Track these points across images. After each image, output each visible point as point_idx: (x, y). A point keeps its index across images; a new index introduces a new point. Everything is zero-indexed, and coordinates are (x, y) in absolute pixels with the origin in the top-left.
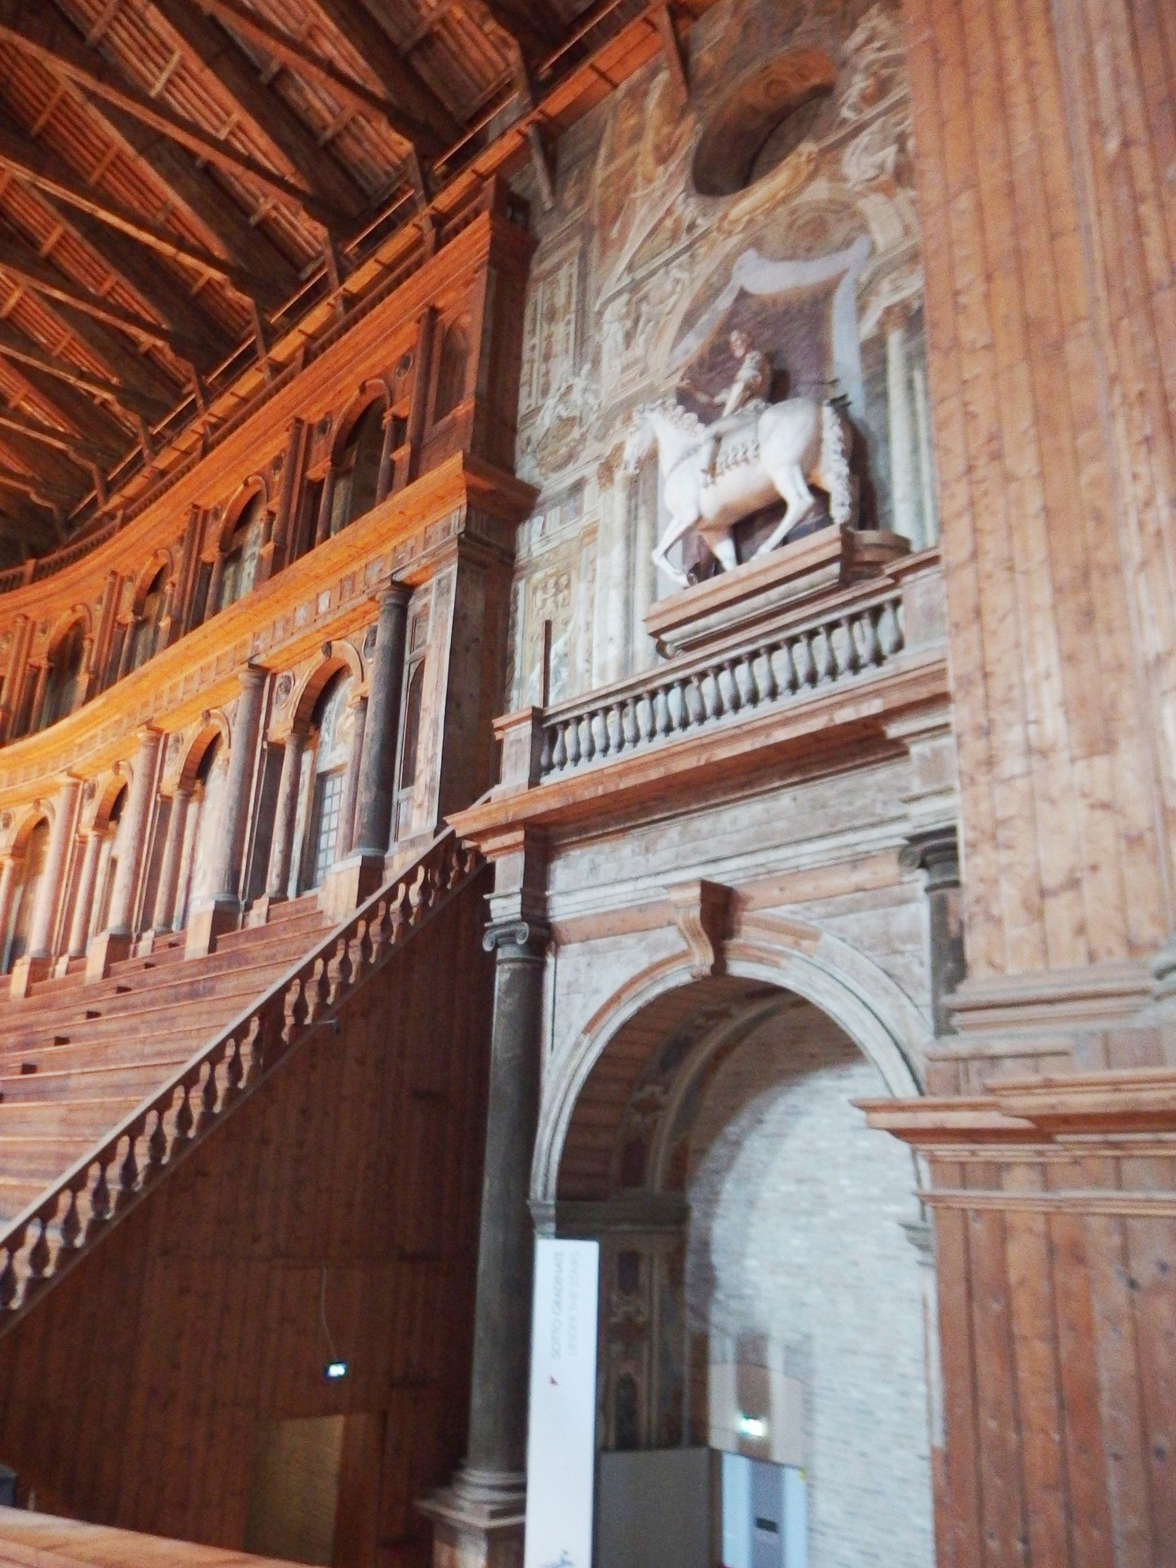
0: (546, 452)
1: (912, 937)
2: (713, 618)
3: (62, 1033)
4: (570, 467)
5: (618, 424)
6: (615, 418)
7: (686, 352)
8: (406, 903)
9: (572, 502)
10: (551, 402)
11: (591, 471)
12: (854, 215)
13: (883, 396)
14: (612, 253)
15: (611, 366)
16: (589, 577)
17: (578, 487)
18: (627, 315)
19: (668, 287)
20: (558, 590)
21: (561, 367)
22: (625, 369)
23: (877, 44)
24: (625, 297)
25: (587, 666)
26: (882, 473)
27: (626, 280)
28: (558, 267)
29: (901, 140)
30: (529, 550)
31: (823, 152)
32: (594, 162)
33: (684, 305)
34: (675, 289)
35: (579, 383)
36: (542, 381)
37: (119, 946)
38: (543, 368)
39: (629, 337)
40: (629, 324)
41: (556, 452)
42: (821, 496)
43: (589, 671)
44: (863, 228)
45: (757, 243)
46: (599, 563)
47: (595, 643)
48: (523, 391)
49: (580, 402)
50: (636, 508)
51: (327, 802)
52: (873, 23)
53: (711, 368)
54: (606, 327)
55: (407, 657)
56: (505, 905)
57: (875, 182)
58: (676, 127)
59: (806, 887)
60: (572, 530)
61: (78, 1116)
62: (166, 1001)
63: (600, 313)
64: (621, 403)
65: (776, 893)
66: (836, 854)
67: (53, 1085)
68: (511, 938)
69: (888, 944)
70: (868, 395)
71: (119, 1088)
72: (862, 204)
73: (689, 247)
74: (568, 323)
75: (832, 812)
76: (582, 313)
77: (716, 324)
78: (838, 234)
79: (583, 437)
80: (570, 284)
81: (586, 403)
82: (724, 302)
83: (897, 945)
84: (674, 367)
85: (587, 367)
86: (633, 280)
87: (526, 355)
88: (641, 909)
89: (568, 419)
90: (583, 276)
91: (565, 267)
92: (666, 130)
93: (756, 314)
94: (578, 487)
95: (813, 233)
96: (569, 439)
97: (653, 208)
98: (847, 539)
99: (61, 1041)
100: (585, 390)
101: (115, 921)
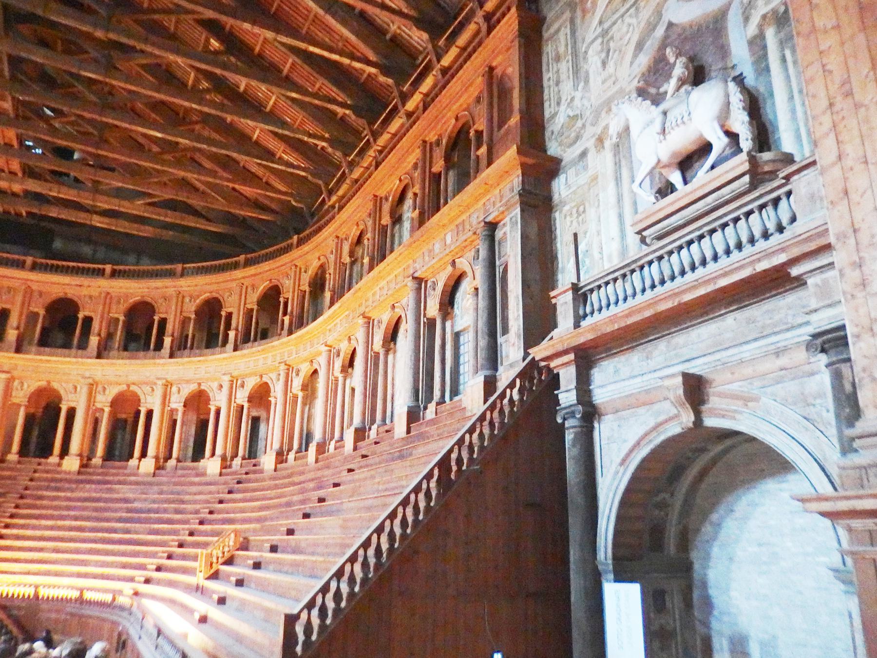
1: (821, 395)
3: (336, 481)
5: (603, 114)
7: (639, 65)
8: (511, 400)
10: (563, 108)
13: (767, 69)
14: (588, 16)
15: (595, 81)
16: (596, 204)
17: (584, 154)
18: (602, 51)
20: (579, 215)
21: (567, 87)
22: (603, 82)
24: (600, 40)
25: (600, 256)
26: (771, 116)
27: (599, 30)
28: (558, 31)
33: (635, 38)
34: (629, 29)
37: (360, 434)
38: (556, 89)
39: (604, 64)
40: (603, 55)
41: (569, 136)
42: (733, 137)
43: (602, 258)
46: (601, 195)
47: (603, 242)
48: (546, 105)
49: (579, 106)
51: (462, 348)
55: (497, 263)
56: (567, 396)
59: (748, 371)
61: (350, 524)
62: (387, 461)
63: (586, 52)
65: (729, 375)
66: (766, 349)
67: (334, 508)
68: (572, 415)
69: (805, 401)
70: (756, 70)
71: (369, 509)
74: (568, 61)
75: (760, 324)
76: (575, 54)
77: (656, 47)
79: (584, 126)
82: (660, 32)
83: (810, 400)
85: (582, 84)
88: (647, 392)
90: (573, 32)
93: (680, 35)
94: (584, 154)
98: (752, 160)
99: (336, 485)
101: (357, 421)
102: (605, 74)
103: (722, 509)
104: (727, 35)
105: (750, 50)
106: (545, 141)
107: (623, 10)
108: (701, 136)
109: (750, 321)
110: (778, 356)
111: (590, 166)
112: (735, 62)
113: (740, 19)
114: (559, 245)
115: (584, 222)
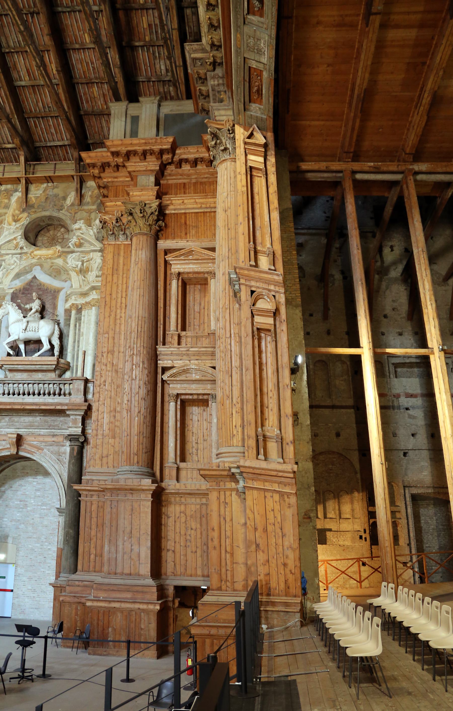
1: (65, 453)
2: (20, 366)
7: (16, 284)
12: (68, 274)
13: (69, 325)
19: (13, 262)
26: (66, 344)
29: (83, 262)
31: (63, 252)
33: (17, 270)
45: (41, 266)
52: (81, 225)
53: (23, 293)
58: (21, 213)
59: (41, 439)
69: (59, 454)
70: (65, 323)
72: (70, 272)
73: (20, 254)
77: (26, 281)
78: (64, 277)
82: (29, 277)
83: (61, 454)
84: (12, 287)
92: (17, 212)
93: (38, 285)
95: (57, 272)
97: (10, 234)
98: (58, 359)
103: (7, 486)
104: (58, 301)
112: (58, 314)
113: (64, 299)
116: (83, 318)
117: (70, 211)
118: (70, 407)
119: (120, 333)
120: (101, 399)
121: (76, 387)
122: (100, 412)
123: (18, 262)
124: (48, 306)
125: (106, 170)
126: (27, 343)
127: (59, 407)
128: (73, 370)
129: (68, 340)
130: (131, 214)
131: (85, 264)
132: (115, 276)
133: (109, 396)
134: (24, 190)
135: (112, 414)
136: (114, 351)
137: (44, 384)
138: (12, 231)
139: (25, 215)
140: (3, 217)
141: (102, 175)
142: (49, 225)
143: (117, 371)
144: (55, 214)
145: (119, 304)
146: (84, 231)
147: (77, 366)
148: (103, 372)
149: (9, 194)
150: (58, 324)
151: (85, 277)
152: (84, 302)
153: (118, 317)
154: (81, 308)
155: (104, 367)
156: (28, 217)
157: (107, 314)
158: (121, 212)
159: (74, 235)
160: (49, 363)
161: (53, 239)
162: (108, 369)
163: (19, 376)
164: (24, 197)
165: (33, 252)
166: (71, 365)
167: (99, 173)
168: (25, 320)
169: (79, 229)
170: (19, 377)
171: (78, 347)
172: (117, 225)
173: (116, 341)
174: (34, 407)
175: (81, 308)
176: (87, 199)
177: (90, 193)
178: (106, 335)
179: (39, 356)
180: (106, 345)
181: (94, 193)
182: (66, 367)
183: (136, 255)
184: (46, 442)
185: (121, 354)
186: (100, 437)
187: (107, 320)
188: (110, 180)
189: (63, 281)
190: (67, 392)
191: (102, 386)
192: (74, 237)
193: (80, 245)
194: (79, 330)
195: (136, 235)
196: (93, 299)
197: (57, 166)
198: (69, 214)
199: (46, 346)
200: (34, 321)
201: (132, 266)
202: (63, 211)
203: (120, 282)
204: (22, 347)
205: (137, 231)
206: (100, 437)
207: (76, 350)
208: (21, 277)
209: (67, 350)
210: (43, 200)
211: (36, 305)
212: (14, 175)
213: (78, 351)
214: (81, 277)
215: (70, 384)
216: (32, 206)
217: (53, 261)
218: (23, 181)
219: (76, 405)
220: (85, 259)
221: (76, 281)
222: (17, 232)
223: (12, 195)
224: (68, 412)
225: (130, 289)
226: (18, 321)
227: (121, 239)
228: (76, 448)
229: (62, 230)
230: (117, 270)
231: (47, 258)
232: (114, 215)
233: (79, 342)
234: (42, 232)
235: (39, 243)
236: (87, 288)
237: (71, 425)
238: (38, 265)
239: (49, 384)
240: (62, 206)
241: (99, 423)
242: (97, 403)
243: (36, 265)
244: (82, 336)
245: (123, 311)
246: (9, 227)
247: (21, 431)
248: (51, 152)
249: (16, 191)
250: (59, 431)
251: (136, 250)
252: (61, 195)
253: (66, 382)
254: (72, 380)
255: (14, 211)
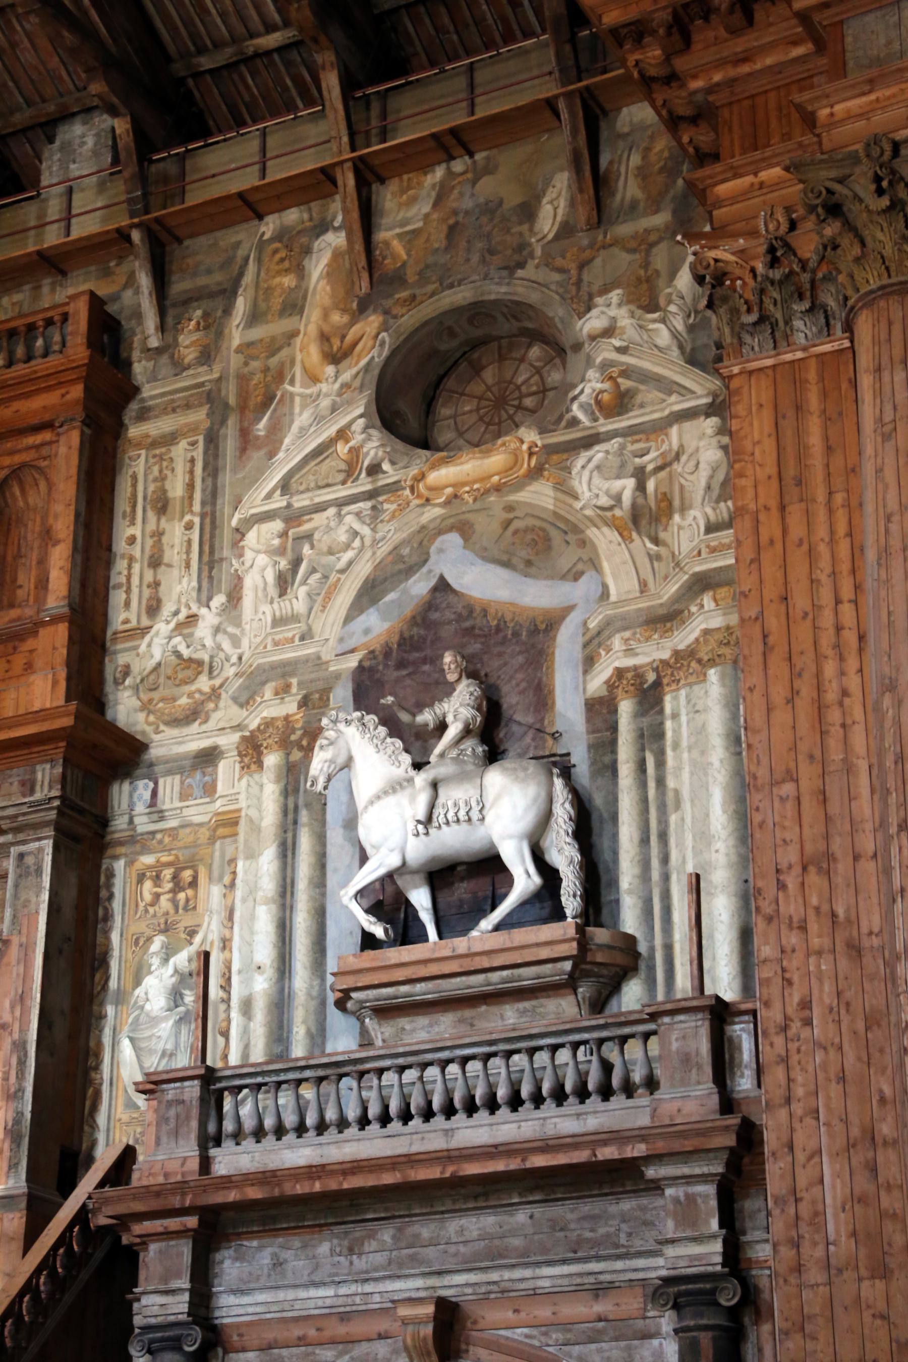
0: (156, 695)
4: (195, 727)
5: (268, 692)
6: (264, 683)
7: (367, 631)
9: (198, 775)
10: (162, 628)
11: (229, 741)
12: (583, 543)
14: (256, 456)
15: (257, 609)
16: (227, 880)
17: (208, 758)
18: (281, 551)
19: (343, 538)
20: (178, 887)
21: (179, 587)
22: (278, 622)
23: (617, 343)
24: (277, 525)
25: (222, 994)
26: (607, 856)
27: (278, 502)
28: (171, 439)
29: (641, 476)
30: (131, 821)
31: (551, 450)
32: (228, 311)
33: (364, 569)
34: (352, 541)
35: (208, 618)
36: (147, 593)
38: (149, 576)
39: (284, 583)
40: (284, 564)
41: (174, 699)
42: (550, 875)
43: (227, 1001)
44: (594, 564)
45: (464, 529)
46: (240, 864)
47: (235, 967)
48: (117, 598)
49: (209, 642)
50: (296, 809)
52: (613, 312)
53: (400, 665)
54: (249, 555)
57: (609, 514)
58: (352, 323)
59: (544, 1312)
60: (199, 812)
64: (273, 667)
65: (510, 1314)
66: (579, 1280)
70: (593, 763)
72: (592, 533)
73: (371, 495)
74: (189, 527)
75: (574, 1235)
76: (211, 521)
77: (408, 610)
78: (566, 559)
79: (215, 694)
80: (191, 472)
81: (219, 648)
82: (419, 587)
84: (351, 644)
85: (219, 600)
86: (289, 506)
87: (120, 546)
88: (344, 1317)
89: (190, 660)
90: (213, 470)
91: (183, 444)
92: (337, 318)
93: (460, 618)
94: (208, 758)
95: (535, 545)
96: (193, 688)
97: (319, 419)
100: (217, 630)
102: (284, 607)
104: (551, 668)
105: (589, 720)
106: (101, 681)
107: (343, 492)
108: (493, 846)
109: (556, 1226)
110: (597, 1296)
111: (220, 788)
112: (559, 726)
113: (578, 653)
114: (115, 937)
115: (190, 907)
116: (669, 725)
117: (559, 262)
118: (661, 1146)
119: (849, 769)
120: (800, 1092)
121: (675, 1046)
122: (801, 1157)
123: (366, 531)
124: (513, 700)
125: (696, 37)
126: (441, 875)
127: (608, 1153)
128: (652, 968)
129: (615, 836)
130: (834, 210)
131: (651, 485)
132: (795, 512)
133: (833, 1070)
134: (355, 215)
135: (859, 1157)
136: (830, 857)
137: (531, 1052)
138: (325, 403)
139: (373, 321)
140: (284, 353)
141: (681, 64)
142: (476, 344)
143: (855, 950)
144: (496, 290)
145: (827, 639)
146: (628, 337)
147: (668, 948)
148: (794, 963)
149: (294, 249)
150: (567, 772)
151: (656, 541)
152: (666, 655)
153: (831, 696)
154: (658, 684)
155: (793, 939)
156: (384, 327)
157: (779, 693)
158: (788, 210)
159: (589, 362)
160: (544, 953)
161: (500, 402)
162: (815, 942)
163: (419, 1032)
164: (359, 246)
165: (422, 476)
166: (642, 948)
167: (668, 59)
168: (421, 779)
169: (609, 332)
170: (423, 1035)
171: (665, 860)
172: (777, 274)
173: (834, 808)
174: (499, 1166)
175: (658, 684)
176: (628, 189)
177: (635, 160)
178: (788, 789)
179: (497, 928)
180: (792, 834)
181: (653, 158)
182: (620, 959)
183: (878, 393)
184: (565, 1325)
185: (868, 867)
186: (814, 1275)
187: (782, 716)
188: (717, 78)
189: (563, 577)
190: (637, 1076)
191: (795, 1027)
192: (592, 374)
193: (620, 403)
194: (661, 782)
195: (870, 299)
196: (706, 632)
197: (479, 77)
198: (557, 277)
199: (524, 880)
200: (462, 777)
201: (869, 450)
202: (529, 271)
203: (822, 532)
204: (420, 898)
205: (872, 279)
206: (814, 1275)
207: (655, 875)
208: (385, 593)
209: (614, 883)
210: (439, 240)
211: (459, 708)
212: (309, 163)
213: (666, 878)
214: (642, 545)
215: (647, 1036)
216: (398, 279)
217: (512, 498)
218: (348, 180)
219: (683, 1135)
220: (650, 460)
221: (620, 570)
222: (349, 403)
223: (307, 251)
224: (651, 1172)
225: (871, 555)
226: (394, 787)
227: (800, 339)
228: (705, 1339)
229: (535, 352)
230: (799, 482)
231: (487, 492)
232: (753, 233)
233: (663, 836)
234: (451, 383)
235: (444, 435)
236: (673, 588)
237: (670, 1228)
238: (450, 529)
239: (554, 1048)
240: (522, 247)
241: (805, 1210)
242: (783, 1114)
243: (440, 532)
244: (678, 805)
245: (852, 663)
246: (313, 390)
247: (456, 1285)
248: (446, 20)
249: (322, 227)
250: (619, 1265)
251: (879, 370)
252: (513, 198)
253: (627, 1030)
254: (654, 1017)
255: (326, 315)
